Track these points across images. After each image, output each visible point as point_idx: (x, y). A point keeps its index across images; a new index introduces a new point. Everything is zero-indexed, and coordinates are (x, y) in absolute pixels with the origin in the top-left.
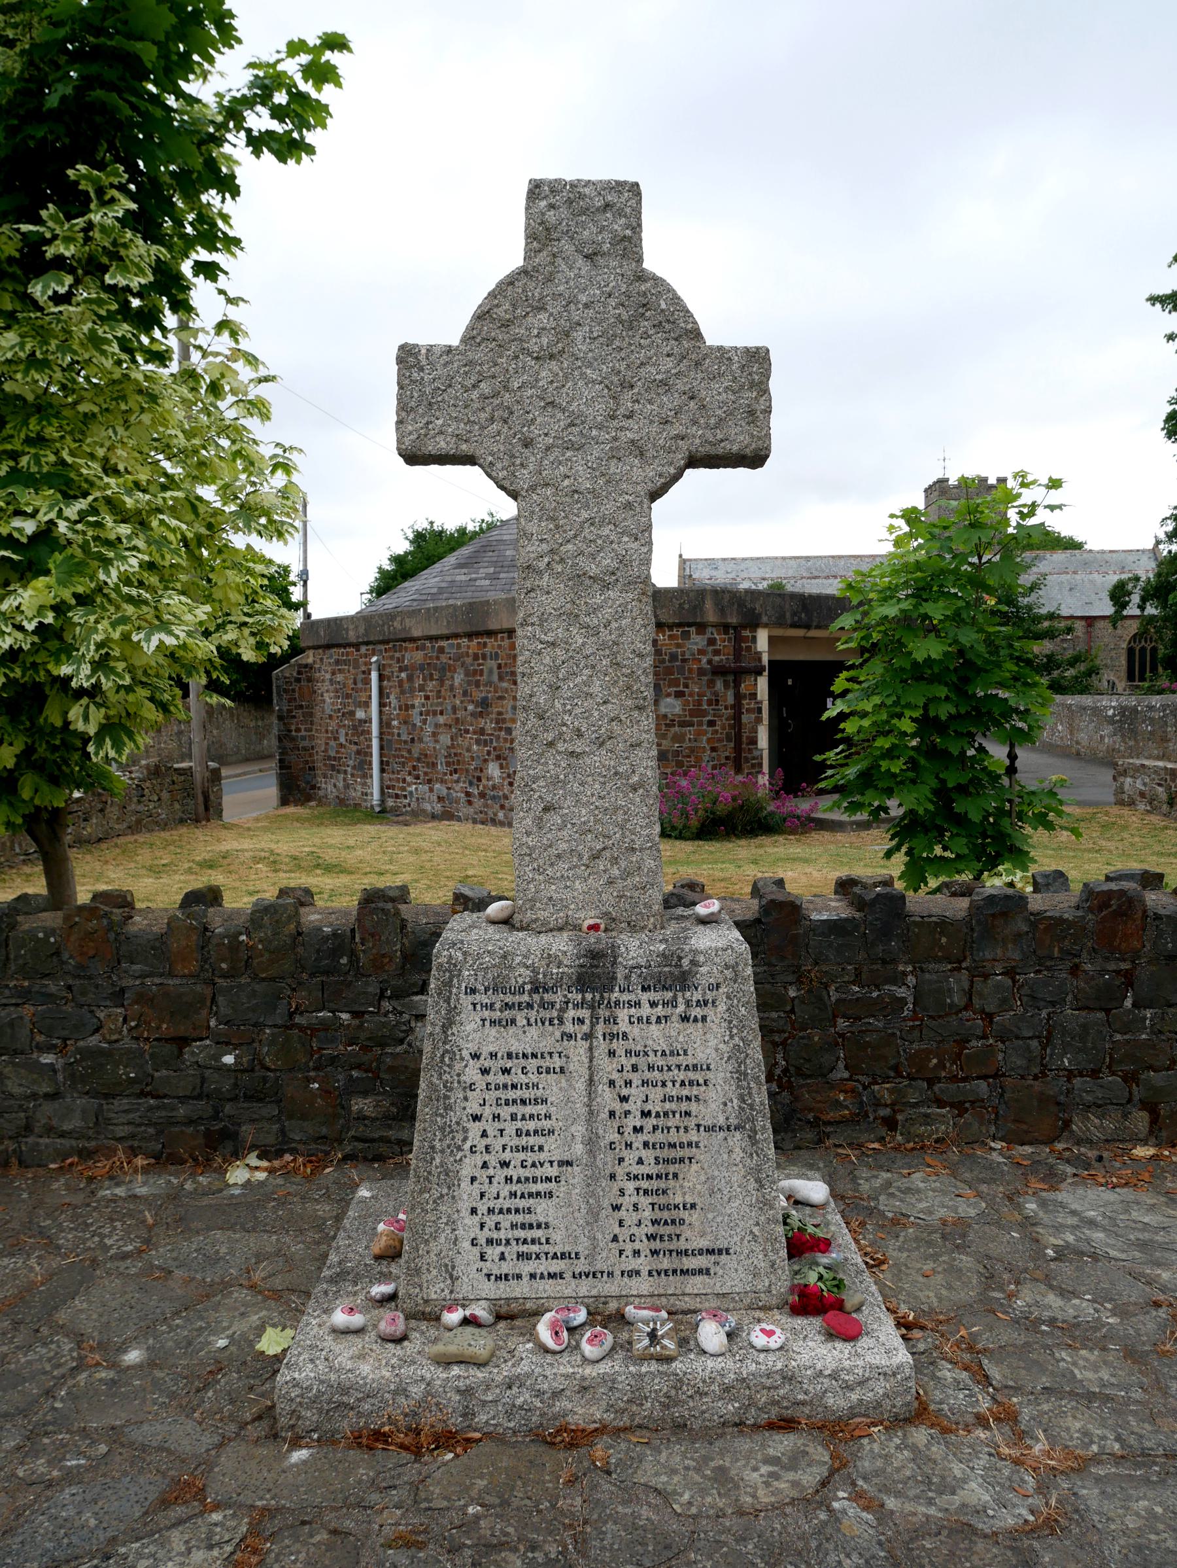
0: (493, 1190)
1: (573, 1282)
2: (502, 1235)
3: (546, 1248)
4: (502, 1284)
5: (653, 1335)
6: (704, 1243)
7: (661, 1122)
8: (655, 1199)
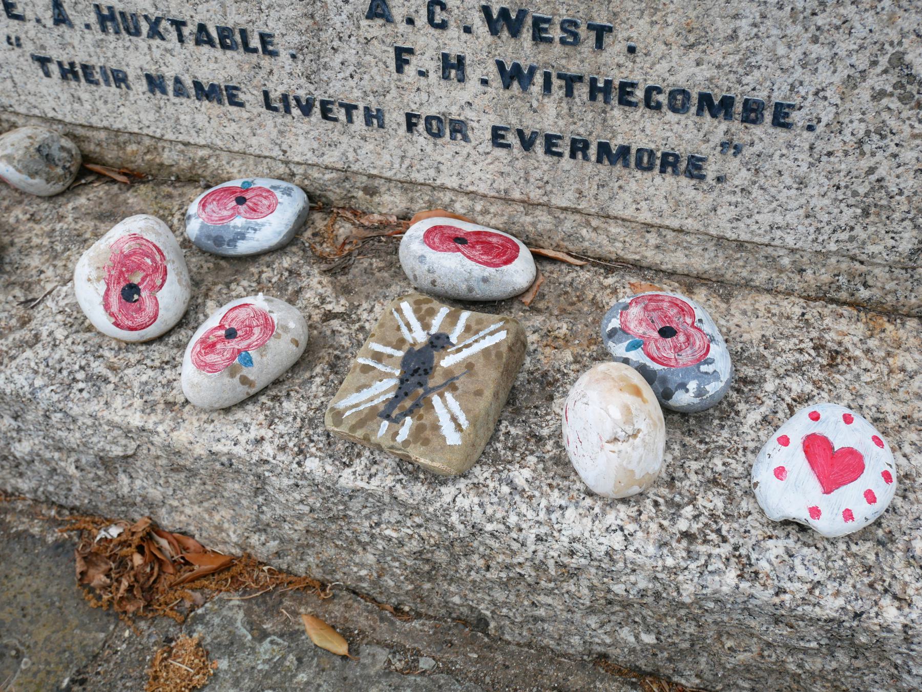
1: (271, 121)
5: (418, 368)
6: (690, 74)
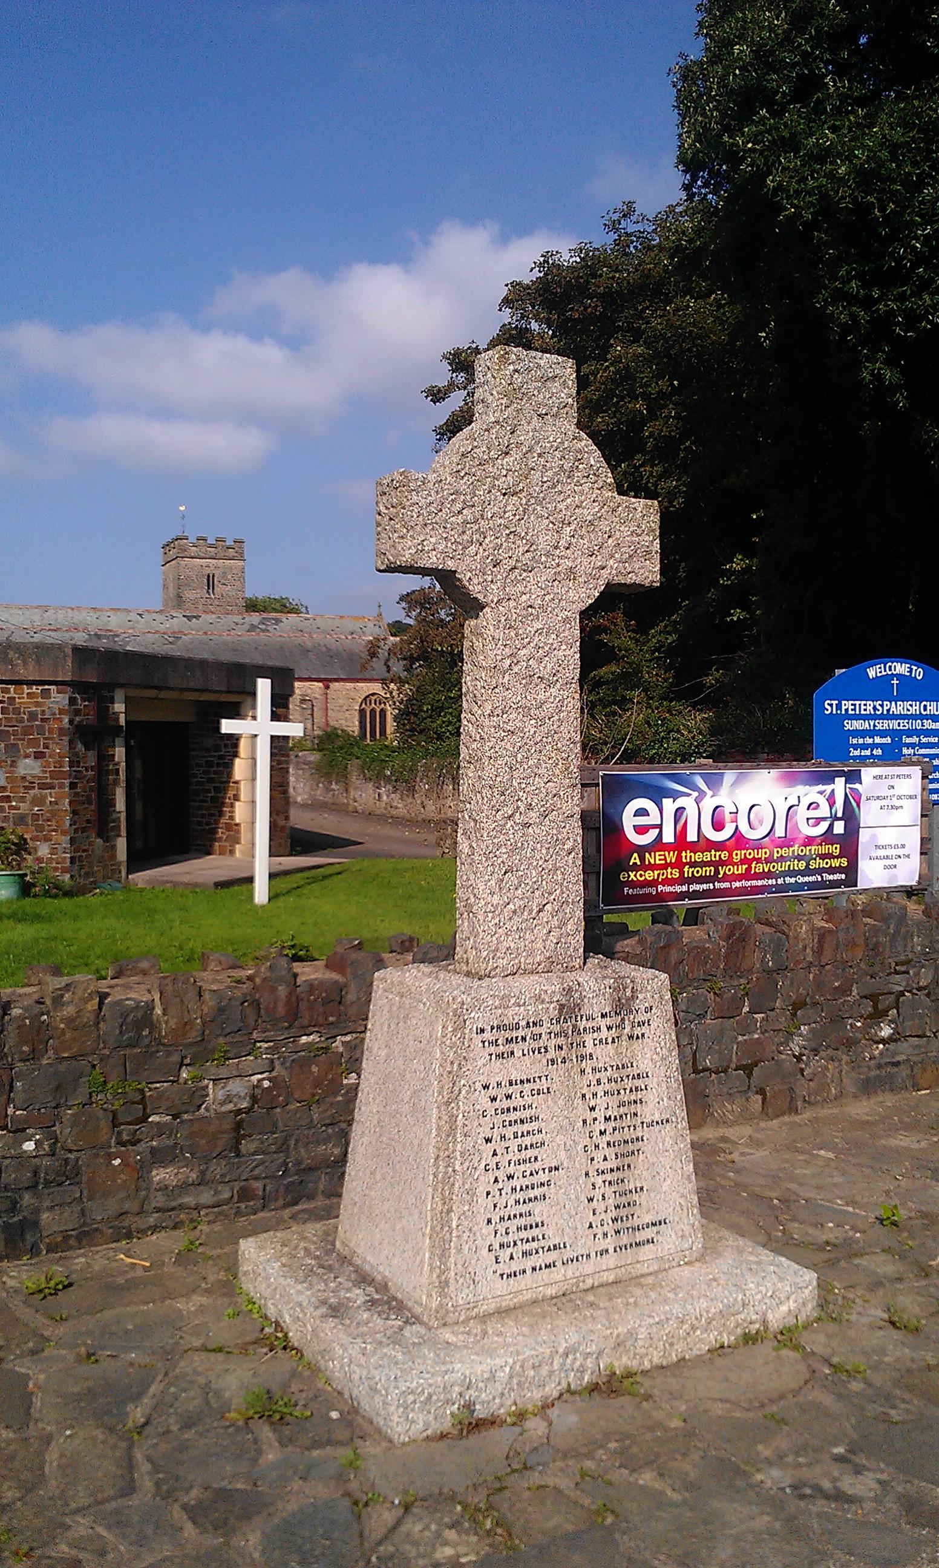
0: (502, 1203)
2: (510, 1238)
3: (542, 1243)
4: (512, 1280)
7: (618, 1124)
8: (614, 1188)
